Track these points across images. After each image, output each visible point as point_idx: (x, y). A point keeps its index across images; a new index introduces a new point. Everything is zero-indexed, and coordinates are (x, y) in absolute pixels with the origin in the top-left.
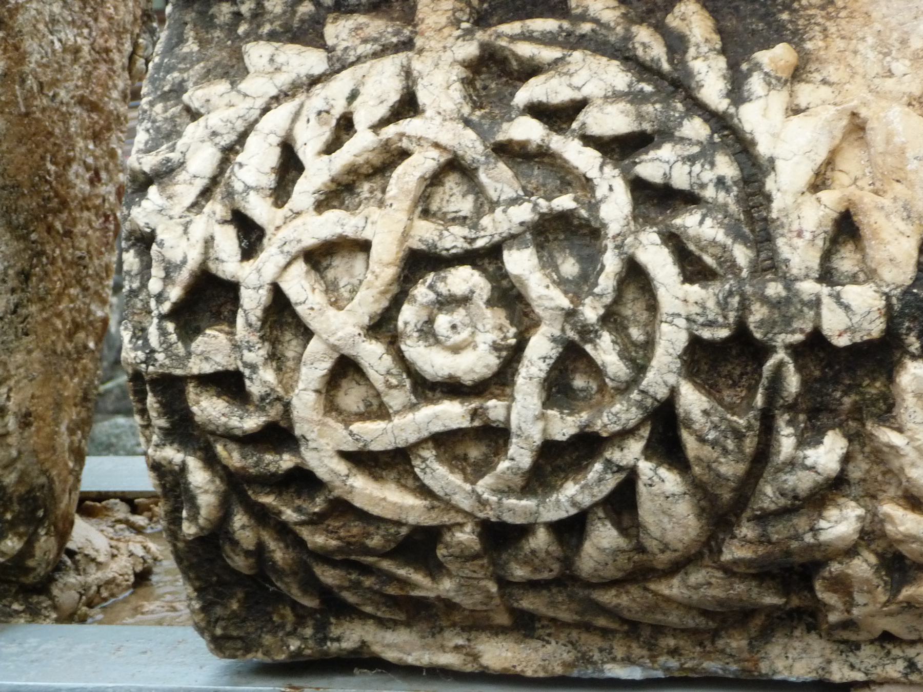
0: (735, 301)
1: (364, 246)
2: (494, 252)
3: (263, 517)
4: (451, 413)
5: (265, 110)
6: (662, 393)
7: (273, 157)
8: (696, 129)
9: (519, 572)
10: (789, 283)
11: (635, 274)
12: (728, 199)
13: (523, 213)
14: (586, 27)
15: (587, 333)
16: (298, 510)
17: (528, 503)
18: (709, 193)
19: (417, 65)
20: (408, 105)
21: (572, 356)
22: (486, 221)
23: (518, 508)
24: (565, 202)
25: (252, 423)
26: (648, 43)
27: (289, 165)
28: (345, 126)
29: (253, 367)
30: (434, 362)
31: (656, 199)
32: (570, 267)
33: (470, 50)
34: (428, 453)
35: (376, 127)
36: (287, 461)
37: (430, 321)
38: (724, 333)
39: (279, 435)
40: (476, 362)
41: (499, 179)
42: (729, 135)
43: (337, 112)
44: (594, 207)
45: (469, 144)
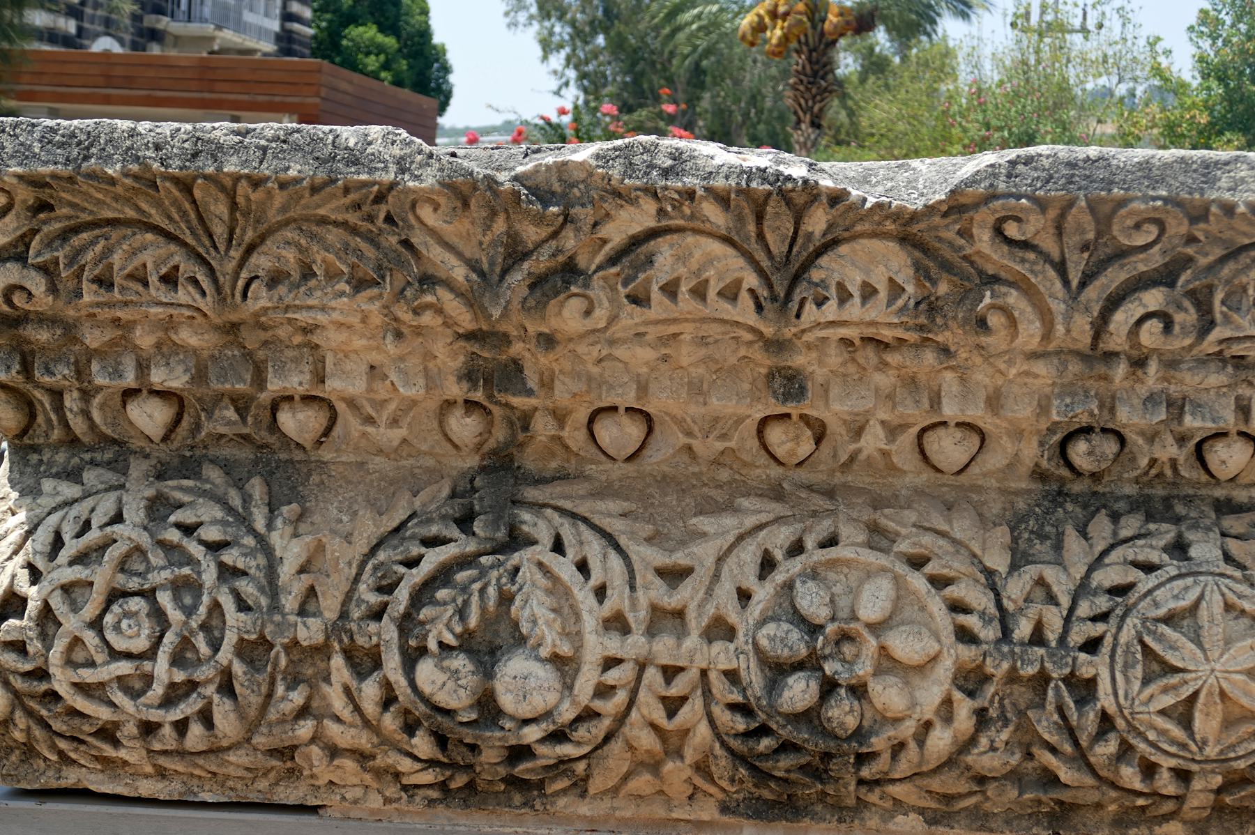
0: (259, 622)
1: (91, 584)
2: (153, 590)
3: (30, 713)
4: (124, 668)
5: (49, 513)
6: (225, 663)
7: (50, 538)
8: (249, 541)
9: (157, 746)
10: (284, 615)
11: (216, 606)
12: (260, 575)
13: (166, 574)
14: (208, 486)
15: (192, 632)
16: (49, 711)
17: (161, 712)
18: (252, 571)
19: (125, 499)
20: (118, 518)
21: (186, 642)
22: (150, 576)
23: (155, 715)
24: (186, 571)
25: (28, 667)
26: (235, 500)
27: (58, 542)
28: (87, 526)
29: (31, 639)
30: (119, 644)
31: (228, 573)
32: (188, 600)
33: (150, 492)
34: (115, 685)
35: (101, 527)
36: (43, 687)
37: (119, 622)
38: (254, 637)
39: (41, 674)
40: (140, 644)
41: (157, 558)
42: (264, 546)
43: (83, 518)
44: (199, 573)
45: (145, 540)
